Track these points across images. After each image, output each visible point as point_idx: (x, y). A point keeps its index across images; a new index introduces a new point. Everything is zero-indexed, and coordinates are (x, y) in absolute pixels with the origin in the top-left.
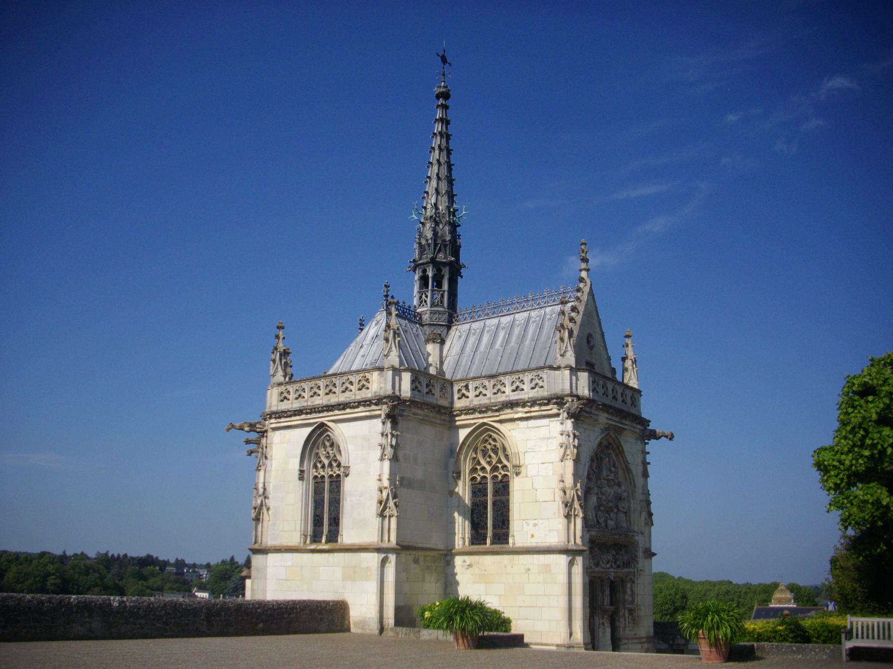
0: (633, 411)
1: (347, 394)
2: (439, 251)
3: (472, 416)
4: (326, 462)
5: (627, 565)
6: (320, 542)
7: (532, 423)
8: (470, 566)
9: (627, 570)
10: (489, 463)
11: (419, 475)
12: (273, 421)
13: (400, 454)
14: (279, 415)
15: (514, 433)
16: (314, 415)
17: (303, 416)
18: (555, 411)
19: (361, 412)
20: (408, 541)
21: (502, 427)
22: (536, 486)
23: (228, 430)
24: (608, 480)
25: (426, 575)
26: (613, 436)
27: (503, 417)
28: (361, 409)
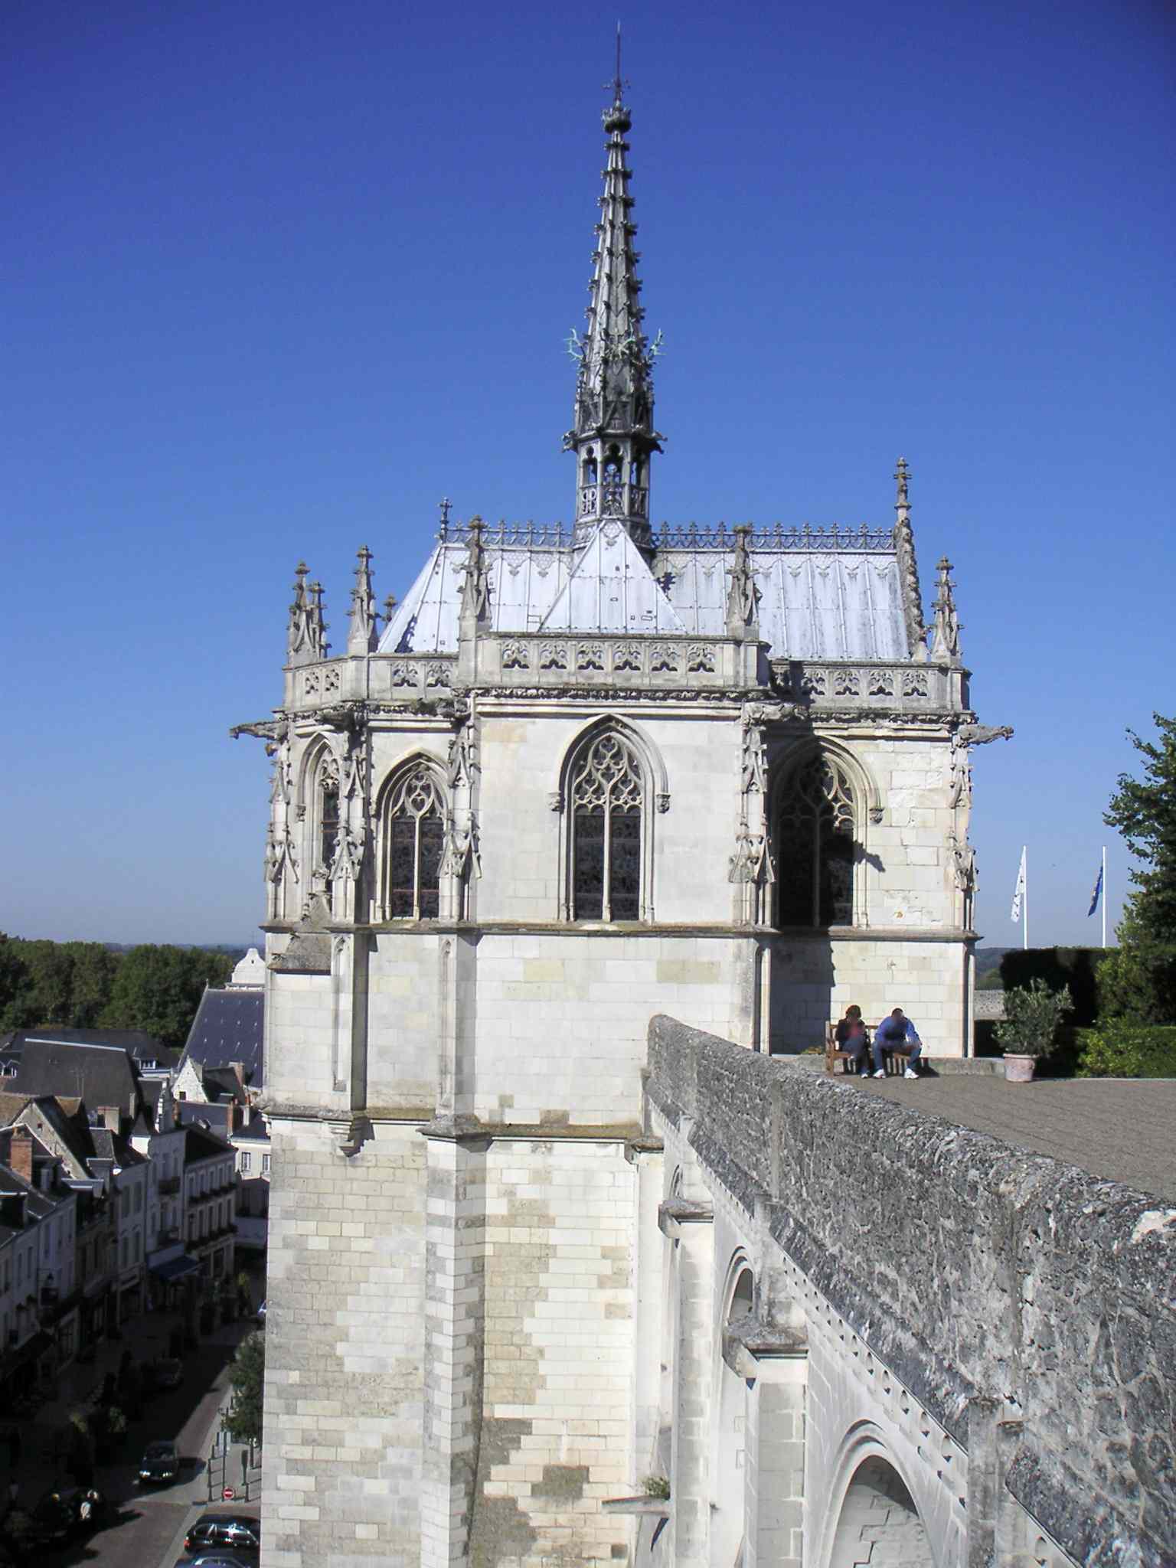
6: (599, 917)
8: (790, 956)
14: (503, 692)
18: (945, 734)
19: (698, 707)
21: (853, 746)
28: (701, 702)
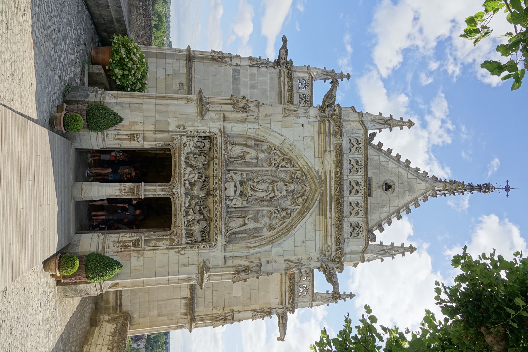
0: (347, 229)
5: (190, 235)
9: (184, 232)
13: (255, 70)
24: (273, 190)
26: (316, 196)
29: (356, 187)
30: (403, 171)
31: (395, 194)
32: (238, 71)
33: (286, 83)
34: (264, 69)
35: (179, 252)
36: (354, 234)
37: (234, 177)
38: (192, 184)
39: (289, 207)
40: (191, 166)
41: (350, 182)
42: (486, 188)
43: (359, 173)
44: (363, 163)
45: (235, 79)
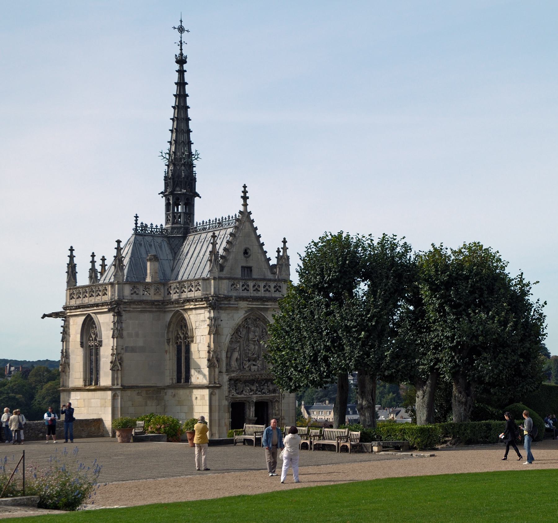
1: (99, 297)
2: (176, 186)
3: (173, 306)
4: (93, 336)
7: (199, 311)
9: (273, 395)
10: (183, 334)
11: (140, 343)
12: (68, 311)
13: (125, 333)
15: (191, 317)
16: (86, 309)
17: (81, 310)
18: (205, 305)
20: (126, 384)
22: (199, 349)
23: (43, 318)
25: (148, 402)
27: (186, 307)
29: (256, 287)
30: (238, 241)
31: (251, 248)
32: (127, 347)
33: (135, 306)
34: (124, 325)
35: (284, 398)
36: (280, 290)
37: (247, 365)
38: (251, 390)
39: (261, 330)
40: (242, 391)
41: (254, 291)
42: (181, 61)
43: (249, 284)
44: (244, 281)
45: (133, 350)
